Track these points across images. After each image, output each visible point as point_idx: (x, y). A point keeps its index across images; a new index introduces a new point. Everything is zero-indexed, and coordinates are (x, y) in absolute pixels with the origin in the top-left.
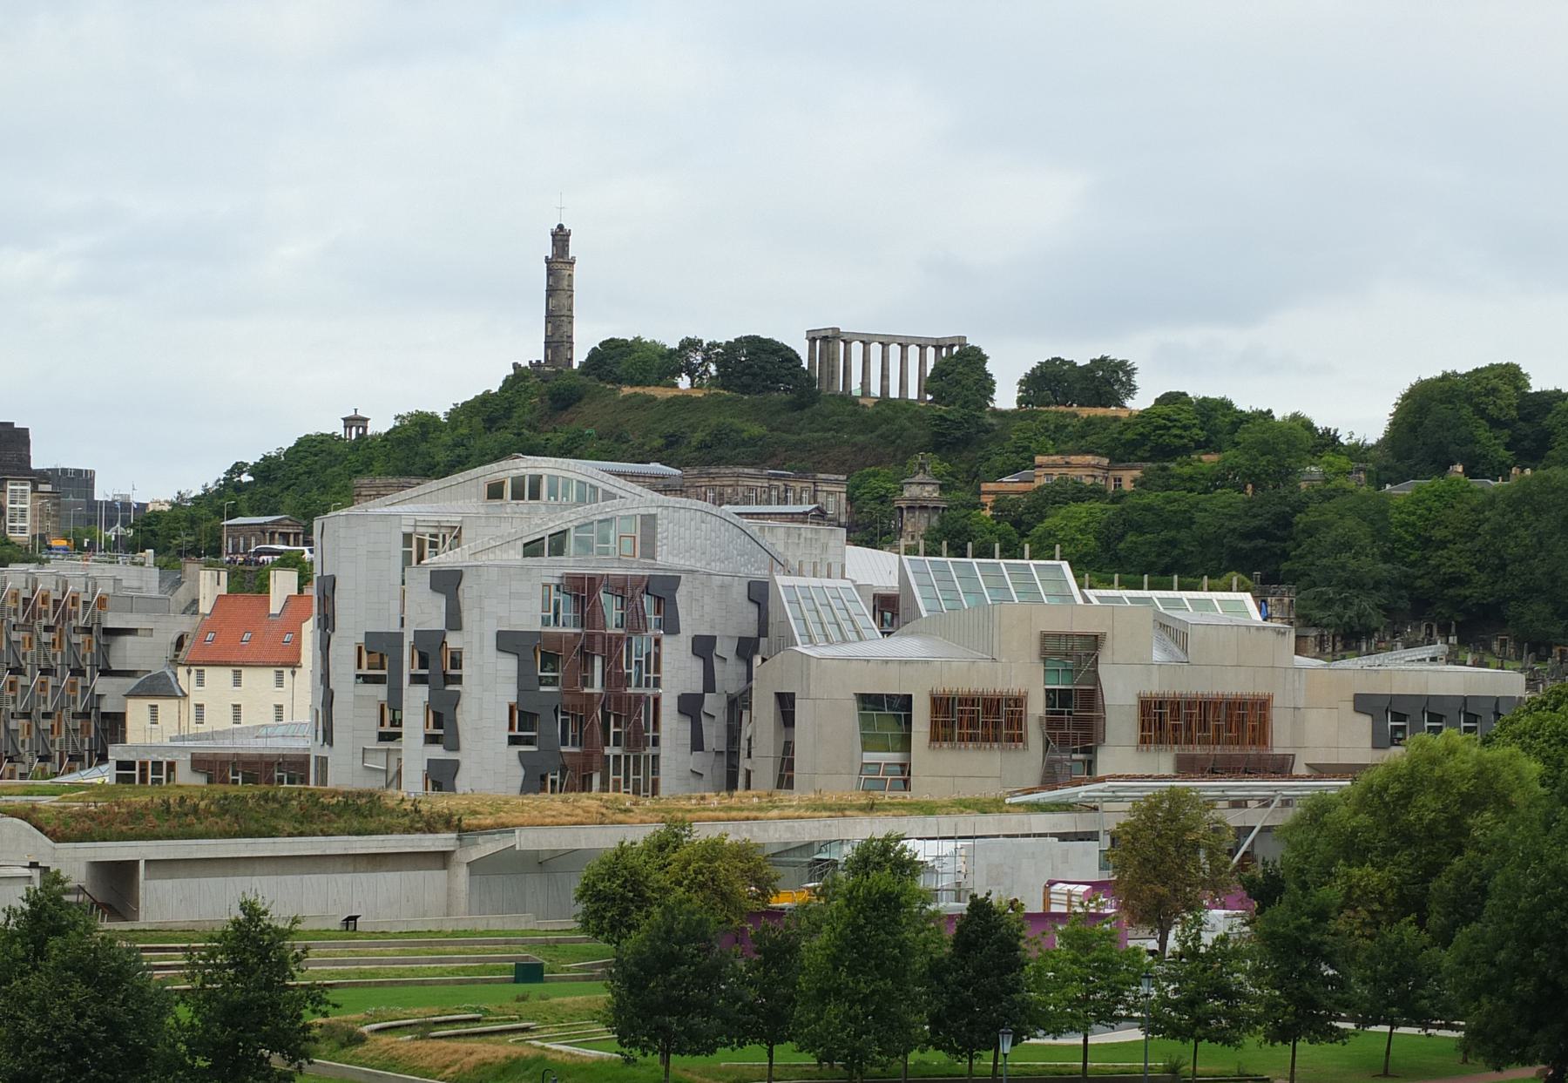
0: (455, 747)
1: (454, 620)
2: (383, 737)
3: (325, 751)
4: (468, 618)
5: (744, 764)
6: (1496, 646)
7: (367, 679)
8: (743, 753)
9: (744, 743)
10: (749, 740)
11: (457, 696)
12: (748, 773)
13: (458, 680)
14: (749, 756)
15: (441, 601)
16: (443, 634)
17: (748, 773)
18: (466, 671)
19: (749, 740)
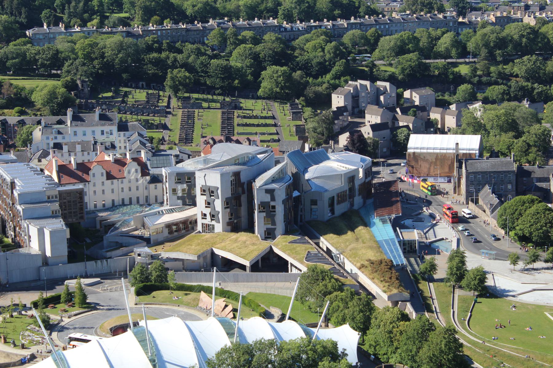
0: (275, 225)
1: (273, 199)
2: (230, 219)
3: (213, 223)
4: (276, 198)
5: (300, 213)
6: (113, 83)
7: (225, 208)
8: (299, 211)
9: (300, 209)
10: (301, 209)
11: (275, 215)
12: (301, 216)
13: (275, 211)
14: (301, 211)
15: (269, 196)
16: (269, 202)
17: (301, 216)
18: (277, 210)
19: (301, 209)
